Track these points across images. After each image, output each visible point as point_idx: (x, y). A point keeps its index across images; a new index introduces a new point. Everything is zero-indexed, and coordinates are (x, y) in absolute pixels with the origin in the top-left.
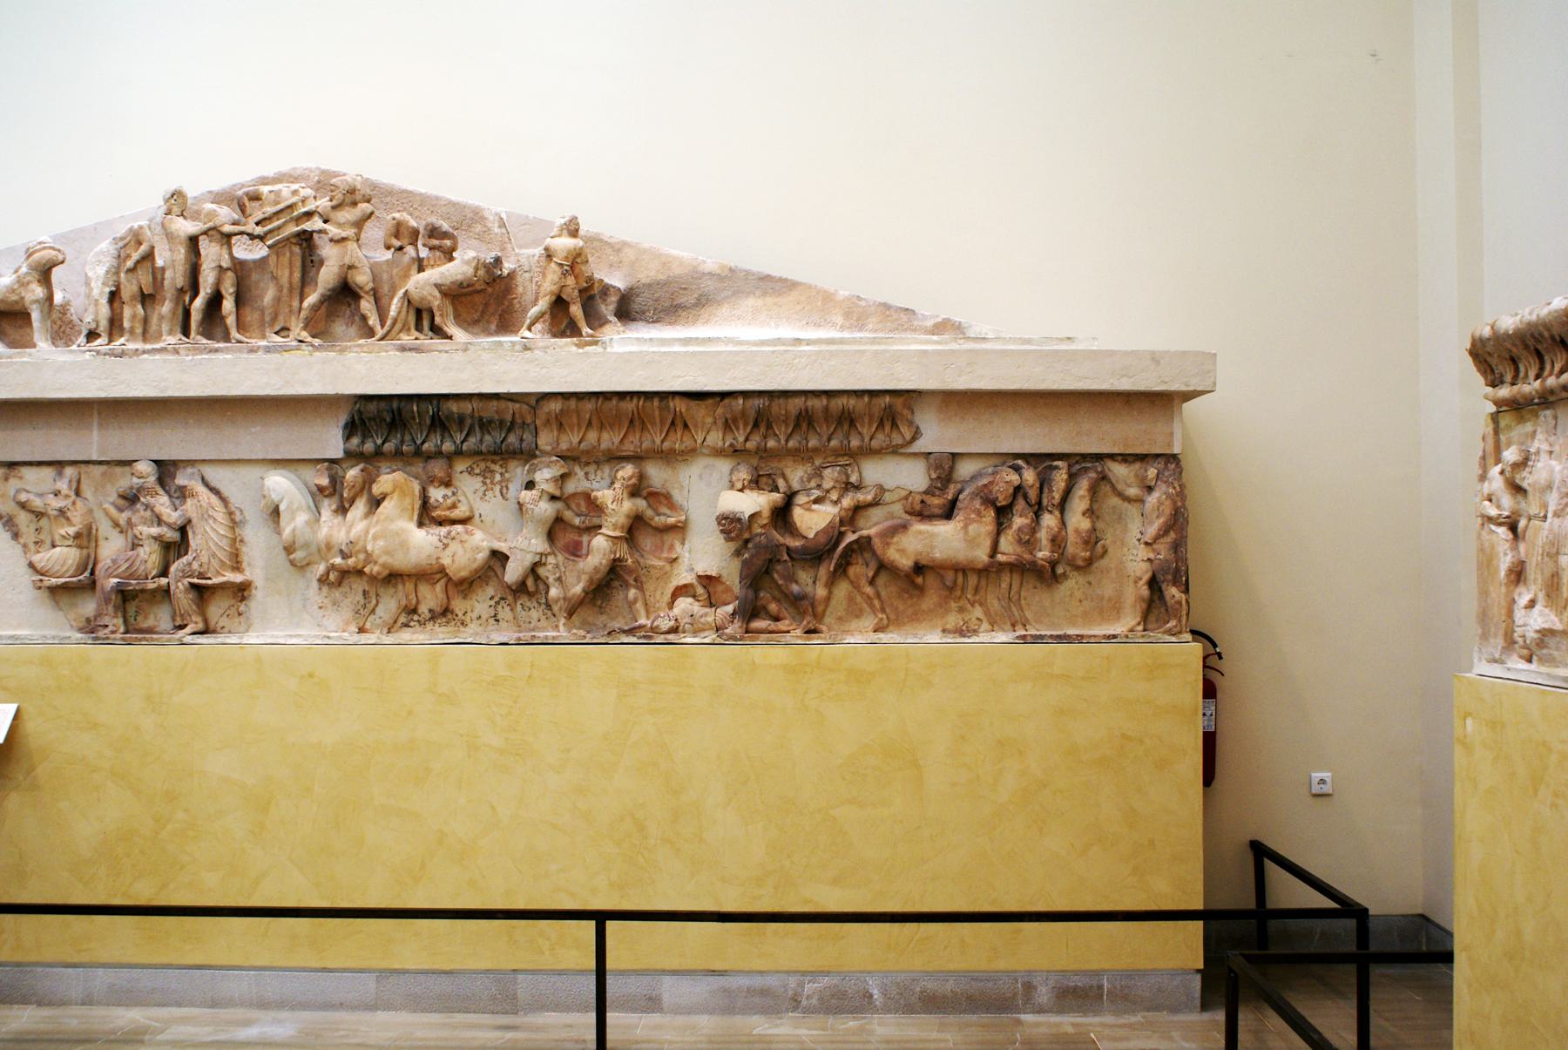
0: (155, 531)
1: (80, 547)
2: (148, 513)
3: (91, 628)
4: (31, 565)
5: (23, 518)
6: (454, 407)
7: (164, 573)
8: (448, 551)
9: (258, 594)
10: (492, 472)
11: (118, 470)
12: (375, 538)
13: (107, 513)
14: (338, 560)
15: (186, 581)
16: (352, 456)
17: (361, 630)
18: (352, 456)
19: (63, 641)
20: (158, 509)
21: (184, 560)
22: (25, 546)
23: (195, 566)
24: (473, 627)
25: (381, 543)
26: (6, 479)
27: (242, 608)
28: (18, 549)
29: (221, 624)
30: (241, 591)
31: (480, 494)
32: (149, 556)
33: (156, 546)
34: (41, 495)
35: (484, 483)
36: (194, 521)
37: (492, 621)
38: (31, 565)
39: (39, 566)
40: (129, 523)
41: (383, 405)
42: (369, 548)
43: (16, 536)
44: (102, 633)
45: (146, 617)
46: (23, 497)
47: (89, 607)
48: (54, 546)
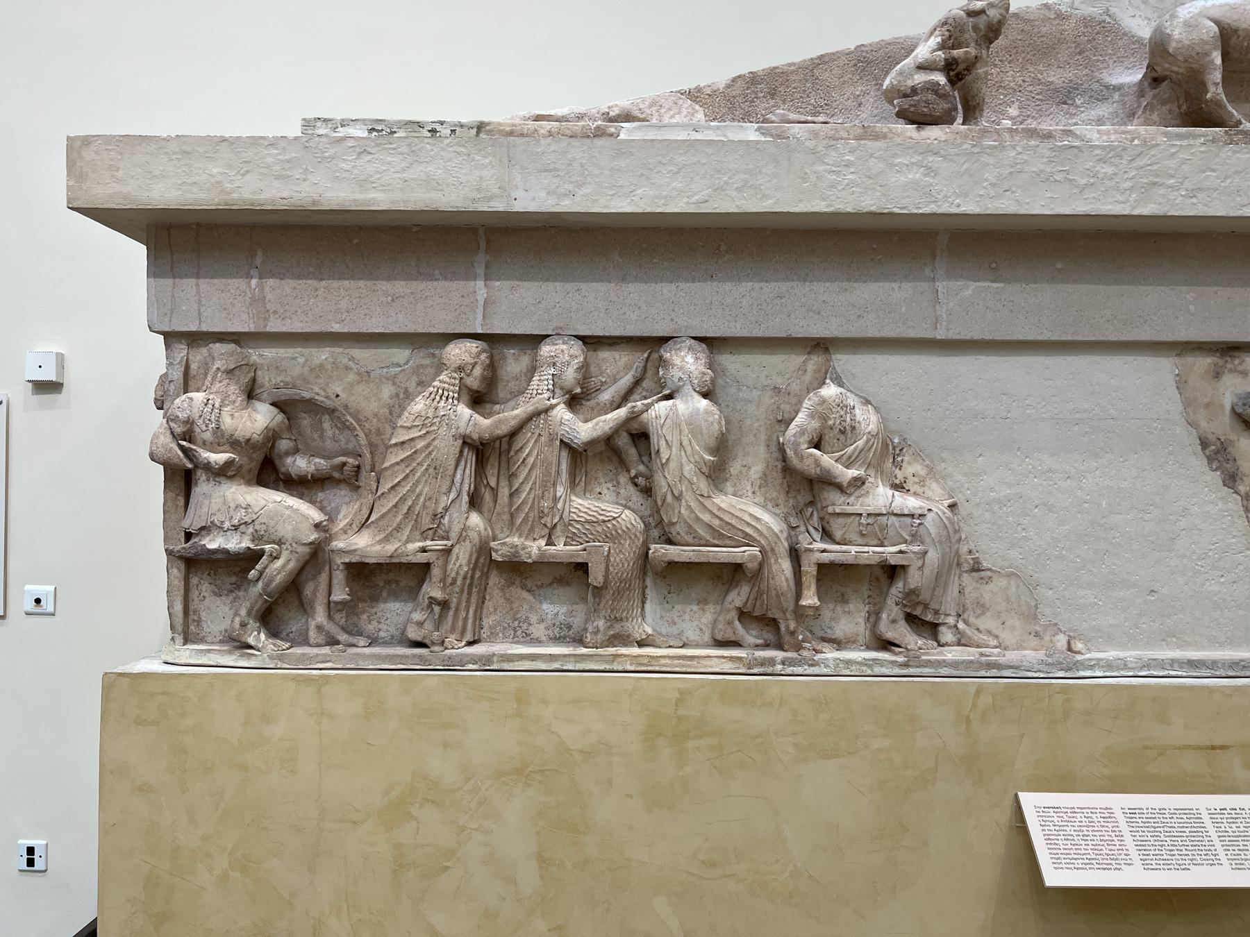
26: (1217, 376)
43: (1231, 479)
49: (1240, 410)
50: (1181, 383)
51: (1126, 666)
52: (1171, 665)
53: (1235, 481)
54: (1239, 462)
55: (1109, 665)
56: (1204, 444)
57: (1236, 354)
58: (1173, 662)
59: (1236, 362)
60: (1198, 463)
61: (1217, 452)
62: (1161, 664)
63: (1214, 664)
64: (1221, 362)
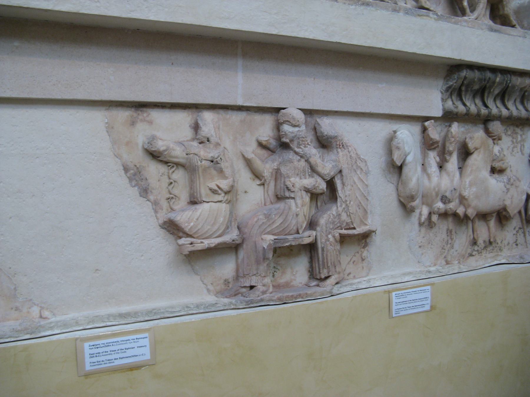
0: (309, 182)
1: (229, 202)
2: (303, 163)
3: (239, 290)
4: (173, 228)
5: (154, 170)
6: (518, 81)
7: (312, 225)
8: (509, 195)
9: (377, 239)
10: (517, 133)
11: (258, 117)
12: (471, 185)
13: (248, 163)
14: (440, 205)
15: (337, 233)
16: (449, 117)
17: (447, 263)
18: (449, 117)
19: (208, 309)
20: (312, 160)
21: (334, 210)
22: (156, 204)
23: (344, 217)
24: (506, 252)
25: (474, 189)
26: (133, 123)
27: (365, 253)
28: (148, 207)
29: (347, 271)
30: (365, 238)
31: (510, 150)
32: (299, 207)
33: (307, 198)
34: (181, 143)
35: (513, 142)
36: (344, 172)
37: (514, 245)
38: (173, 228)
39: (187, 227)
40: (277, 174)
41: (477, 74)
42: (466, 194)
43: (145, 192)
44: (253, 295)
45: (284, 273)
46: (160, 146)
47: (227, 267)
48: (194, 202)
49: (146, 147)
50: (110, 128)
51: (77, 323)
52: (108, 318)
53: (147, 193)
54: (150, 181)
55: (65, 325)
56: (126, 169)
57: (145, 109)
58: (109, 316)
59: (145, 115)
60: (122, 181)
61: (135, 175)
62: (101, 318)
63: (136, 314)
64: (135, 115)
